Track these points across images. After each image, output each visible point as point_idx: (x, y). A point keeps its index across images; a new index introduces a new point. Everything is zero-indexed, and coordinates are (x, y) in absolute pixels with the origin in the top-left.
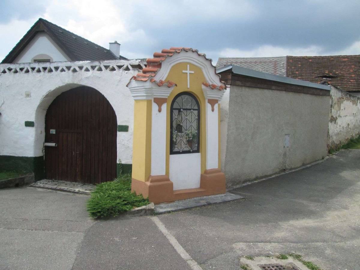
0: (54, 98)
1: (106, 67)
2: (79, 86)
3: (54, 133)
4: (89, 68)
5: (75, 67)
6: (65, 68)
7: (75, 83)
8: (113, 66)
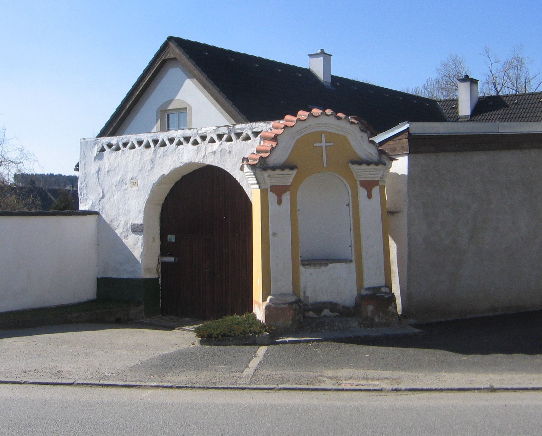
0: (172, 186)
1: (238, 135)
2: (196, 168)
3: (173, 241)
4: (215, 138)
5: (196, 138)
6: (182, 140)
7: (197, 161)
8: (247, 134)
